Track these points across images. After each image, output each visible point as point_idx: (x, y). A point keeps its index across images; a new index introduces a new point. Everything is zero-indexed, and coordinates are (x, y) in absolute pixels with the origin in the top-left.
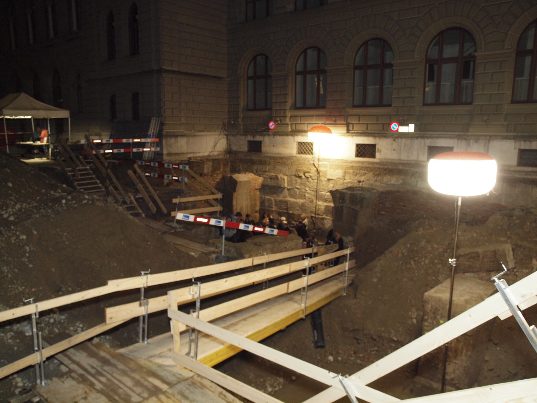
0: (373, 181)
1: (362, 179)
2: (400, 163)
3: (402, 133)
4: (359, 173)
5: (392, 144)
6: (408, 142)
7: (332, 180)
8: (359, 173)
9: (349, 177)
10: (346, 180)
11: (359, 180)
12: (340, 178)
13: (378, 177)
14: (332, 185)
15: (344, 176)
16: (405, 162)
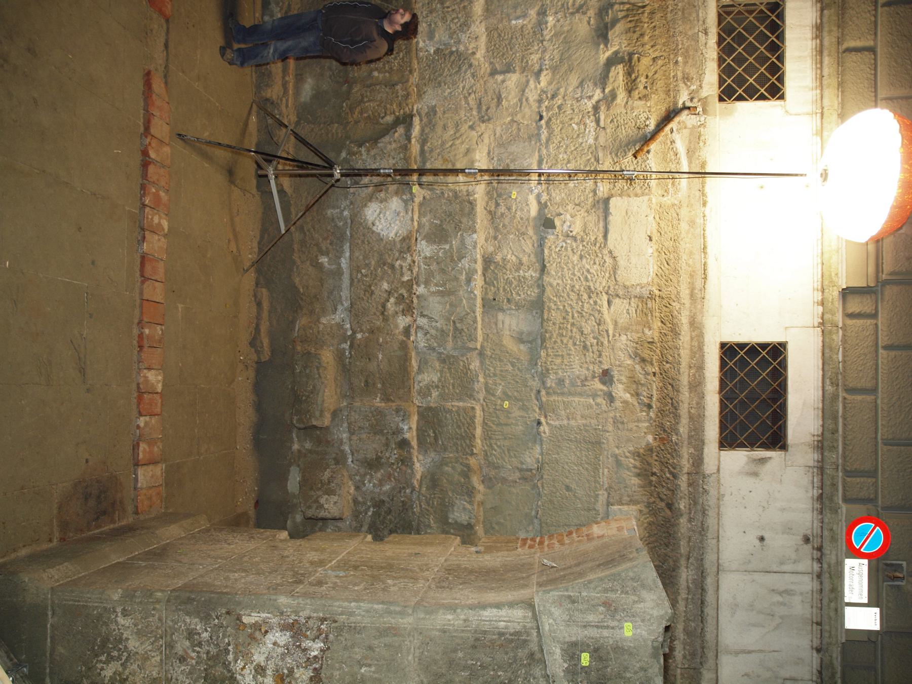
0: (617, 451)
1: (620, 391)
2: (702, 574)
3: (837, 576)
4: (647, 374)
5: (788, 529)
6: (800, 608)
7: (601, 224)
8: (647, 374)
9: (623, 320)
10: (609, 303)
11: (615, 373)
12: (615, 269)
13: (638, 475)
14: (577, 229)
15: (627, 293)
16: (710, 597)
